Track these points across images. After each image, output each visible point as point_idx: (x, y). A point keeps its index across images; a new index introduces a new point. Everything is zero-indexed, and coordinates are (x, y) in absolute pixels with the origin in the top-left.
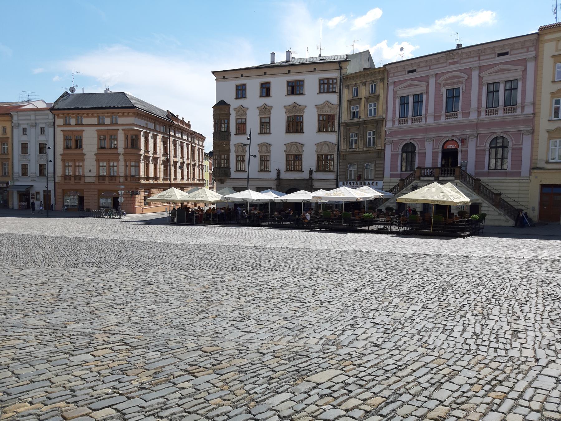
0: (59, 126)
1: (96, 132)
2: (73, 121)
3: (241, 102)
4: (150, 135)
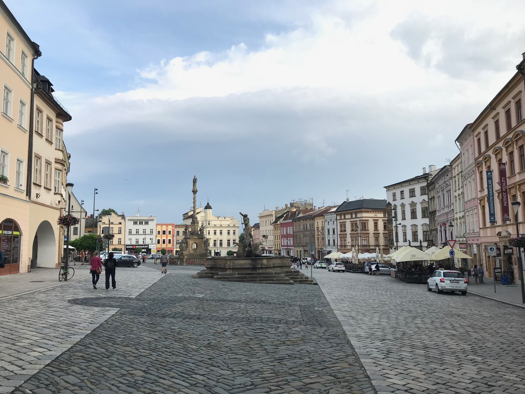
0: (338, 220)
1: (350, 222)
2: (343, 217)
3: (395, 202)
4: (380, 220)
